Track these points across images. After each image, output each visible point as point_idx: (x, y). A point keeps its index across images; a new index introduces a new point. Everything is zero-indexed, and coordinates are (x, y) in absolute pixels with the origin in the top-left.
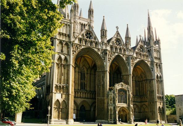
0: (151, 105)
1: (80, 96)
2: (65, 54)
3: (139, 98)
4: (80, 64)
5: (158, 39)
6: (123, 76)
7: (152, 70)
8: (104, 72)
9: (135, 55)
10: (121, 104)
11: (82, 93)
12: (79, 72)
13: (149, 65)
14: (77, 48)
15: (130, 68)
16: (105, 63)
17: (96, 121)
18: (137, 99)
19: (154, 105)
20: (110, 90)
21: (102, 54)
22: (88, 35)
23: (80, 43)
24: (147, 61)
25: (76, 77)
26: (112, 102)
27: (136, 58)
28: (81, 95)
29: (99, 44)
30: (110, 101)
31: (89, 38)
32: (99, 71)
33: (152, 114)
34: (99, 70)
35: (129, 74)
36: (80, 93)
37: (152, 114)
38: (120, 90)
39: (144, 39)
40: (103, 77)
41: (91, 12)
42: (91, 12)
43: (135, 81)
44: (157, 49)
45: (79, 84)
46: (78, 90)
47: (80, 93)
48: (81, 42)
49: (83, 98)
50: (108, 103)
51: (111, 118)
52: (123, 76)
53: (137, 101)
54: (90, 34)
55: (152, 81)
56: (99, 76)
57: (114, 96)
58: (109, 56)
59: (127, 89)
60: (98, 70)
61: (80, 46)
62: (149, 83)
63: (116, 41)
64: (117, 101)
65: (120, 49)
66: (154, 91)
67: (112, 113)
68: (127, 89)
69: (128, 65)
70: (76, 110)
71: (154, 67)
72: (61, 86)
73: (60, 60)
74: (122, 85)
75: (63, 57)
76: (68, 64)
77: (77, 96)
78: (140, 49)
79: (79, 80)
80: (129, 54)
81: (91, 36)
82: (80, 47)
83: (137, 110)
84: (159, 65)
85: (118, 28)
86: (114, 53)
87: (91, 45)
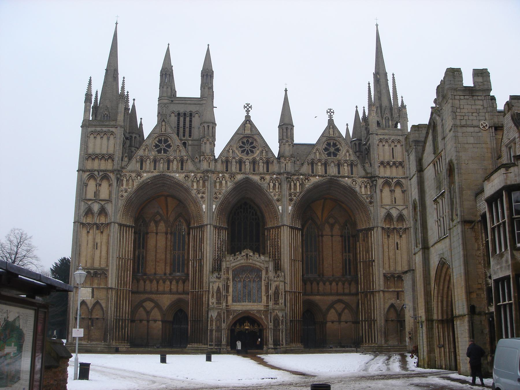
0: (367, 303)
1: (171, 289)
2: (100, 200)
3: (353, 283)
4: (167, 214)
5: (400, 104)
6: (269, 229)
7: (371, 203)
8: (201, 227)
9: (306, 169)
10: (247, 303)
11: (174, 282)
12: (166, 233)
13: (357, 189)
14: (133, 181)
15: (282, 211)
16: (204, 206)
17: (188, 346)
18: (347, 285)
19: (374, 301)
20: (217, 268)
21: (195, 184)
22: (163, 146)
23: (141, 169)
24: (348, 177)
25: (158, 245)
26: (214, 300)
27: (307, 177)
28: (174, 287)
29: (189, 161)
30: (212, 297)
31: (165, 151)
32: (195, 228)
33: (370, 326)
34: (194, 224)
35: (280, 224)
36: (171, 283)
37: (370, 326)
38: (238, 272)
39: (367, 114)
40: (202, 240)
41: (207, 75)
42: (207, 75)
43: (342, 236)
44: (393, 138)
45: (168, 261)
46: (165, 274)
47: (169, 283)
48: (144, 164)
49: (177, 293)
50: (208, 304)
51: (211, 341)
52: (269, 229)
53: (347, 291)
54: (166, 141)
55: (371, 234)
56: (194, 238)
57: (221, 286)
58: (215, 186)
59: (262, 265)
60: (192, 225)
61: (139, 175)
62: (364, 240)
63: (243, 143)
64: (230, 298)
65: (254, 162)
66: (374, 261)
67: (214, 327)
68: (262, 265)
69: (278, 200)
70: (160, 323)
71: (375, 192)
72: (92, 271)
73: (91, 216)
74: (247, 257)
75: (96, 207)
76: (109, 222)
77: (161, 289)
78: (326, 149)
79: (168, 252)
80: (282, 171)
81: (169, 146)
82: (139, 177)
83: (347, 316)
84: (399, 184)
85: (251, 107)
86: (232, 176)
87: (168, 169)
